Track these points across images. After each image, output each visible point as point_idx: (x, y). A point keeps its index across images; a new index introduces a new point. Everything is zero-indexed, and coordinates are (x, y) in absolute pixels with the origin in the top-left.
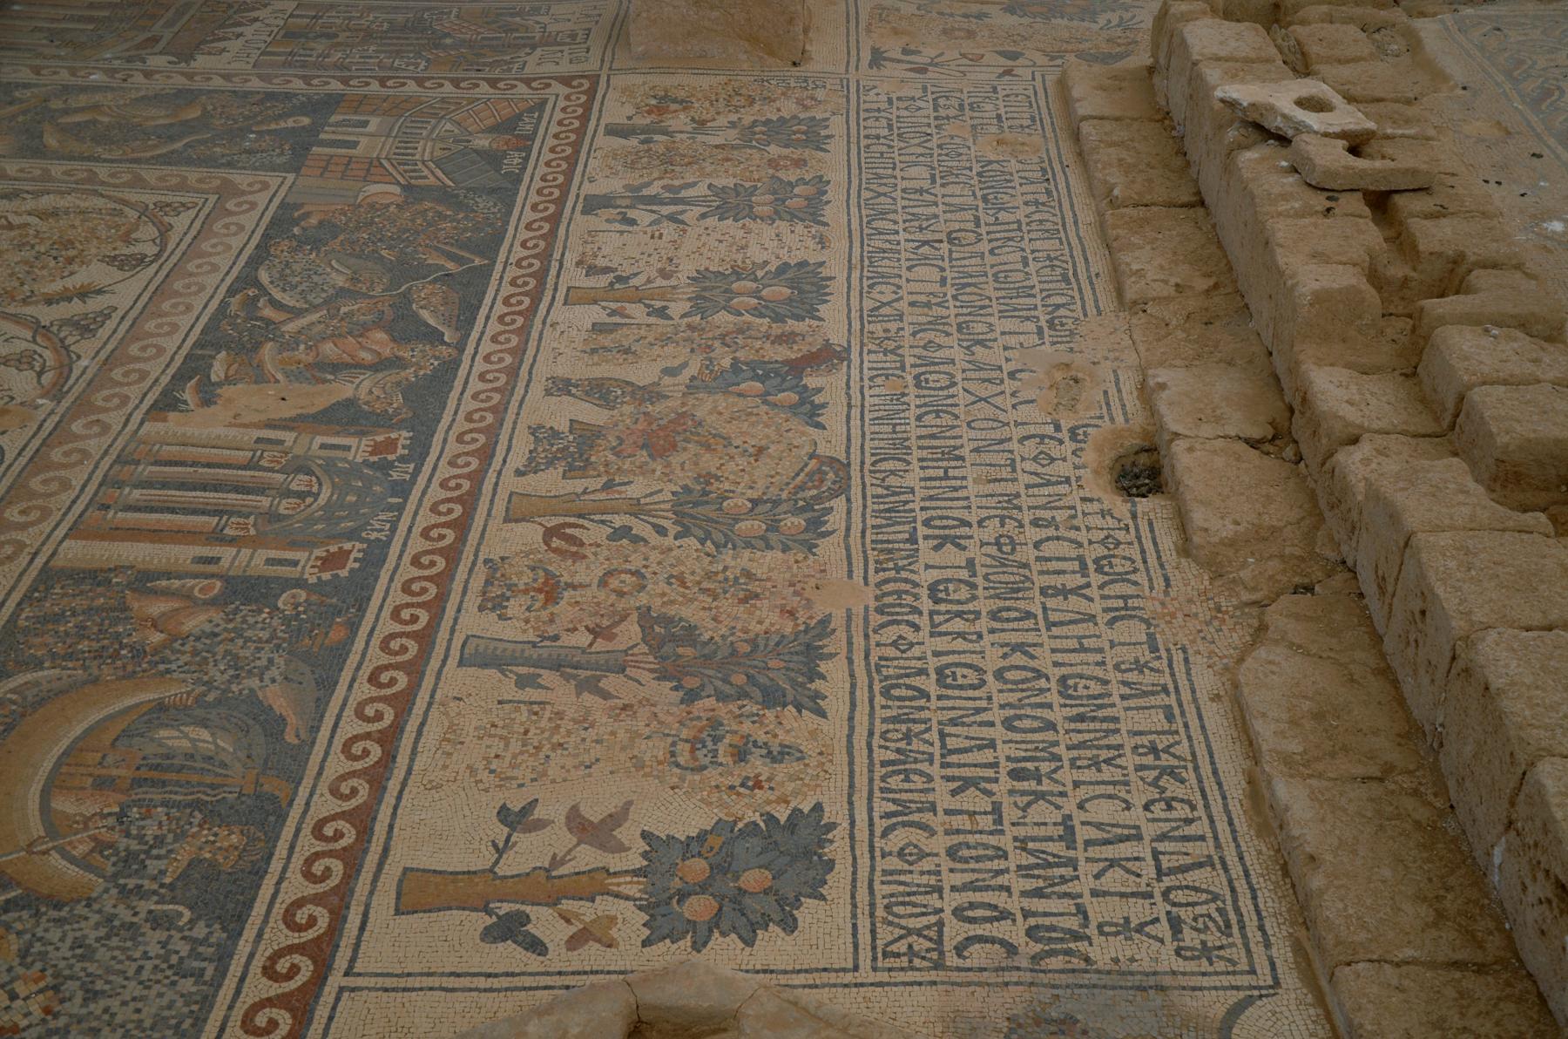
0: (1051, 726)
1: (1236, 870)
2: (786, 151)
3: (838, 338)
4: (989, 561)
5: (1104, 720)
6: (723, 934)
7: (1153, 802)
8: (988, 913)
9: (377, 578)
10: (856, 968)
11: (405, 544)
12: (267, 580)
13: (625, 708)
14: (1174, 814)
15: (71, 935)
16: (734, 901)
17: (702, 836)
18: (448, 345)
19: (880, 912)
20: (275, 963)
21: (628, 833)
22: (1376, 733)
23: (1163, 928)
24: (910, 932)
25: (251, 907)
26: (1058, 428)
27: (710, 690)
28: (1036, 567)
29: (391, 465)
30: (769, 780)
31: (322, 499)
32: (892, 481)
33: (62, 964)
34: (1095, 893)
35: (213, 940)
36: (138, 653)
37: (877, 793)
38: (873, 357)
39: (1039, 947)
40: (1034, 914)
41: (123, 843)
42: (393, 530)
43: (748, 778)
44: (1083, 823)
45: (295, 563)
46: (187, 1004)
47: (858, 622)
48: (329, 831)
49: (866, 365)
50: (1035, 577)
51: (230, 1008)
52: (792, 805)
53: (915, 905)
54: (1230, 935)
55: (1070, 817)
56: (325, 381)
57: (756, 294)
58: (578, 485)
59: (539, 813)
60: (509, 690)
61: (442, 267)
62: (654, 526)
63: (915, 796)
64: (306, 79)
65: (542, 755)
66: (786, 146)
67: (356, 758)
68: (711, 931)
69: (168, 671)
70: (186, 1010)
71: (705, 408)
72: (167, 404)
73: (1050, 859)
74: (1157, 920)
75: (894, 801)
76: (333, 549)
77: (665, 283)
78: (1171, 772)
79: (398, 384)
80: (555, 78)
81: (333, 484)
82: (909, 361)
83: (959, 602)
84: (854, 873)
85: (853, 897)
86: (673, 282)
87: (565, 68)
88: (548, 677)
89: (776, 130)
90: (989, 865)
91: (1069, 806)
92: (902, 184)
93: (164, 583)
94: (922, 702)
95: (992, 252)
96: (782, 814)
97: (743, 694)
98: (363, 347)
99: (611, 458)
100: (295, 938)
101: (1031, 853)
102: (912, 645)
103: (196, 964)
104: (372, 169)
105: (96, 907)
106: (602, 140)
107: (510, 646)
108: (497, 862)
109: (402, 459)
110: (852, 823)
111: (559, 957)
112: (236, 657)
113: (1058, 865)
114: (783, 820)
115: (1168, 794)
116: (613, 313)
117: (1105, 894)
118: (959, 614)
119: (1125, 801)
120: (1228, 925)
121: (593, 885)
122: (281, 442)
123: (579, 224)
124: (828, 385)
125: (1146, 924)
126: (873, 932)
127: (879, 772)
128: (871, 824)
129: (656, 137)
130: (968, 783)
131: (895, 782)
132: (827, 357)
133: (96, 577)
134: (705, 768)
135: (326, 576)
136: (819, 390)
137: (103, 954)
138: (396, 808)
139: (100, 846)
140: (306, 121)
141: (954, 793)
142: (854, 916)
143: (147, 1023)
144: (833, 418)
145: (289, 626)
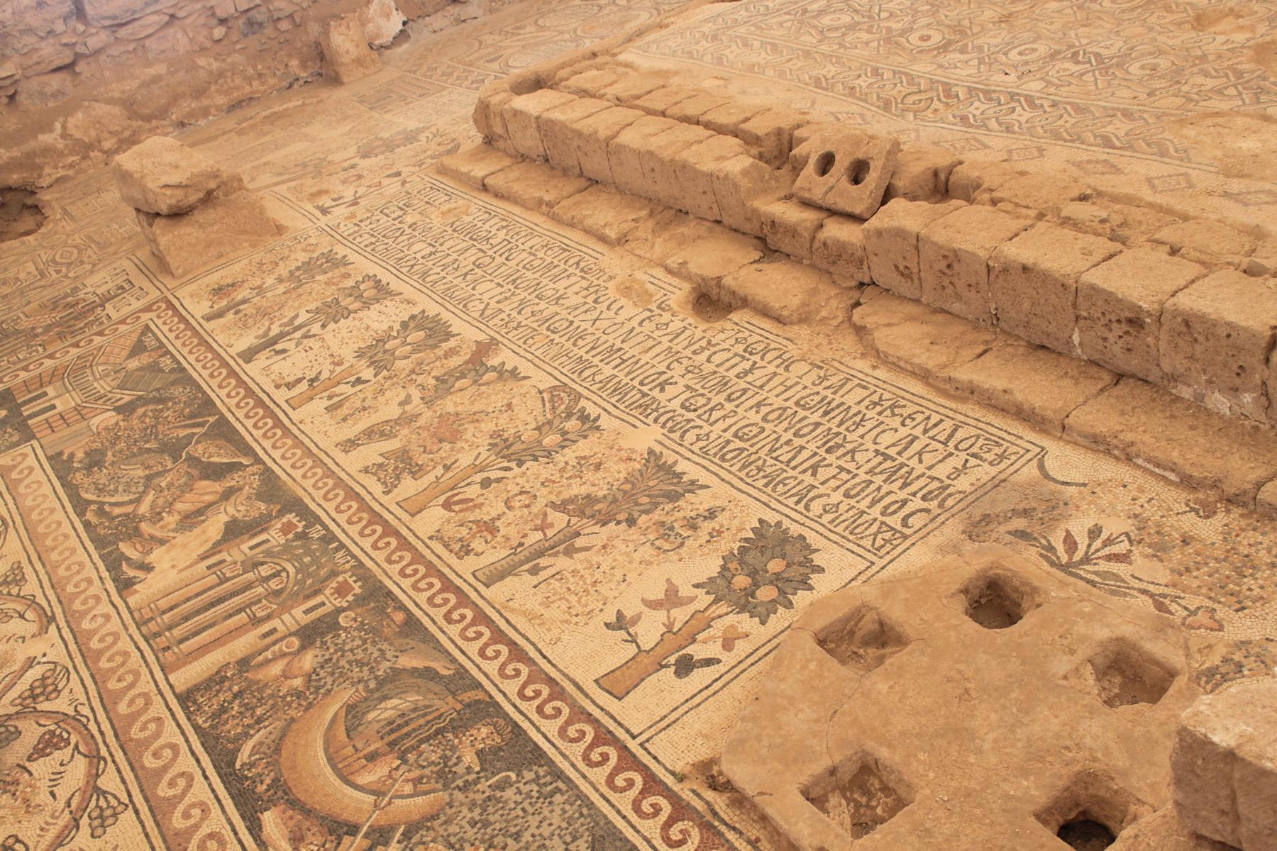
0: (817, 425)
2: (330, 274)
5: (838, 406)
8: (897, 505)
9: (381, 582)
11: (372, 559)
13: (604, 547)
14: (918, 420)
15: (464, 823)
16: (778, 579)
17: (724, 568)
20: (590, 760)
21: (686, 591)
22: (963, 334)
23: (973, 461)
24: (875, 535)
25: (540, 749)
27: (636, 515)
28: (721, 369)
32: (598, 378)
33: (479, 836)
35: (542, 774)
36: (299, 695)
41: (427, 771)
42: (354, 557)
45: (323, 604)
46: (572, 805)
47: (667, 442)
52: (748, 528)
56: (203, 521)
57: (404, 343)
58: (430, 477)
59: (628, 614)
61: (193, 434)
69: (329, 691)
70: (575, 807)
71: (449, 405)
72: (125, 585)
76: (334, 585)
77: (343, 368)
80: (140, 311)
81: (288, 560)
82: (535, 325)
86: (347, 365)
87: (137, 305)
88: (543, 562)
92: (418, 256)
93: (260, 658)
94: (746, 453)
97: (656, 505)
101: (881, 473)
103: (549, 788)
105: (456, 804)
106: (209, 326)
107: (503, 562)
108: (638, 646)
109: (306, 527)
111: (728, 659)
112: (357, 662)
114: (752, 536)
116: (330, 398)
118: (712, 409)
121: (701, 623)
122: (223, 561)
124: (503, 357)
129: (241, 307)
132: (483, 349)
133: (216, 680)
134: (682, 544)
135: (350, 598)
136: (503, 364)
137: (492, 818)
138: (549, 661)
139: (418, 780)
143: (564, 825)
144: (524, 368)
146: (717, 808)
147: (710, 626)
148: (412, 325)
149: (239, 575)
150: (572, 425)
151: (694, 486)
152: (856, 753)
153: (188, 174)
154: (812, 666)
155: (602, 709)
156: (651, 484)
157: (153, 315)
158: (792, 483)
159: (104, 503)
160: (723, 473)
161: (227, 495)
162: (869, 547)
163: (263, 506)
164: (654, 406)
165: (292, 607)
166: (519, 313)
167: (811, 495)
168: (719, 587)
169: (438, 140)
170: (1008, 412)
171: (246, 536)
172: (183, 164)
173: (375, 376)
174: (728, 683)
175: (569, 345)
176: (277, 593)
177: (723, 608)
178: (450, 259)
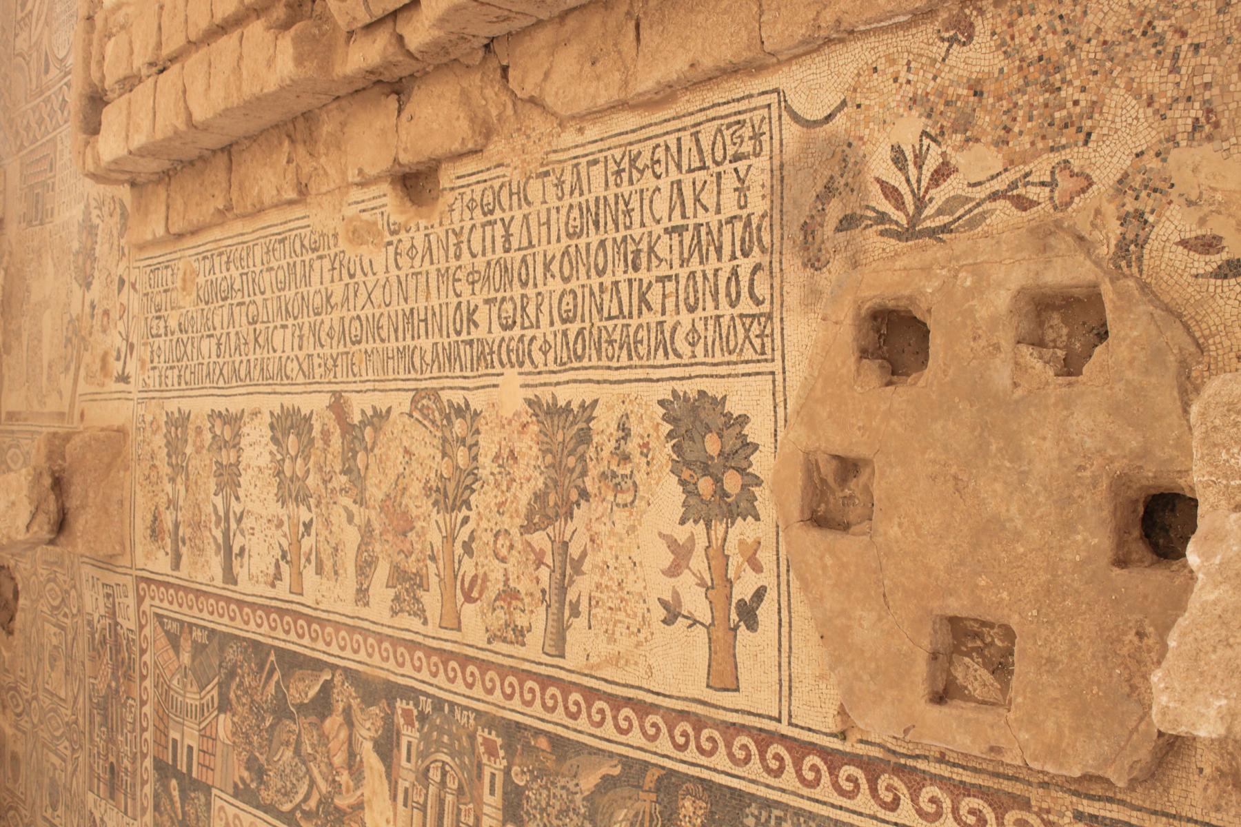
0: (602, 243)
1: (700, 117)
2: (190, 441)
3: (326, 399)
4: (486, 289)
5: (597, 207)
6: (750, 465)
7: (654, 172)
8: (733, 283)
9: (503, 718)
10: (773, 373)
11: (478, 700)
12: (505, 793)
13: (592, 541)
14: (663, 159)
16: (727, 459)
17: (683, 482)
18: (333, 675)
19: (734, 358)
20: (772, 770)
22: (604, 24)
23: (742, 165)
24: (747, 337)
25: (735, 789)
26: (390, 243)
27: (579, 482)
28: (489, 256)
29: (421, 713)
30: (642, 437)
31: (447, 759)
32: (428, 358)
34: (718, 211)
35: (756, 813)
37: (651, 362)
38: (339, 375)
39: (756, 249)
40: (733, 252)
42: (467, 708)
43: (642, 453)
44: (670, 220)
45: (493, 775)
47: (530, 380)
48: (681, 741)
49: (345, 379)
50: (496, 257)
51: (802, 797)
52: (660, 421)
53: (728, 334)
54: (745, 121)
55: (666, 230)
56: (361, 761)
57: (294, 459)
58: (434, 580)
59: (668, 597)
60: (580, 623)
61: (278, 683)
62: (463, 524)
63: (653, 335)
64: (144, 783)
65: (627, 597)
66: (186, 441)
67: (631, 725)
68: (748, 474)
71: (375, 493)
73: (695, 241)
74: (736, 170)
75: (656, 350)
76: (482, 749)
78: (633, 162)
79: (362, 710)
80: (139, 607)
81: (437, 751)
82: (342, 349)
83: (515, 309)
84: (707, 376)
85: (723, 377)
86: (285, 519)
87: (131, 601)
88: (571, 595)
89: (174, 447)
90: (700, 284)
91: (658, 230)
92: (214, 358)
94: (586, 333)
95: (263, 293)
96: (667, 428)
97: (582, 458)
98: (337, 736)
99: (413, 557)
100: (756, 758)
101: (691, 255)
102: (546, 341)
104: (207, 735)
106: (184, 572)
108: (702, 624)
109: (416, 705)
110: (673, 379)
111: (767, 579)
112: (560, 812)
113: (699, 237)
115: (649, 163)
116: (308, 560)
117: (718, 204)
118: (523, 309)
119: (654, 192)
120: (738, 122)
122: (406, 790)
123: (246, 587)
124: (359, 406)
125: (738, 176)
126: (747, 362)
127: (636, 361)
128: (673, 366)
129: (181, 534)
130: (643, 299)
131: (642, 350)
132: (338, 407)
134: (634, 483)
136: (363, 412)
138: (665, 696)
140: (174, 783)
141: (650, 309)
142: (737, 375)
144: (381, 401)
145: (537, 777)
146: (889, 745)
147: (727, 557)
148: (279, 435)
149: (426, 795)
150: (459, 427)
151: (588, 408)
152: (934, 623)
153: (26, 501)
154: (829, 561)
155: (737, 711)
156: (560, 439)
157: (147, 602)
158: (643, 334)
159: (298, 806)
160: (591, 374)
161: (349, 722)
162: (756, 357)
163: (374, 710)
164: (487, 350)
165: (481, 796)
166: (322, 346)
167: (667, 335)
168: (697, 509)
169: (105, 209)
170: (716, 78)
171: (395, 750)
172: (13, 497)
173: (310, 510)
174: (789, 605)
175: (378, 344)
176: (460, 790)
177: (719, 529)
178: (233, 336)
